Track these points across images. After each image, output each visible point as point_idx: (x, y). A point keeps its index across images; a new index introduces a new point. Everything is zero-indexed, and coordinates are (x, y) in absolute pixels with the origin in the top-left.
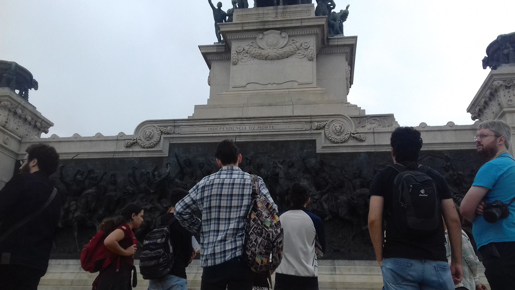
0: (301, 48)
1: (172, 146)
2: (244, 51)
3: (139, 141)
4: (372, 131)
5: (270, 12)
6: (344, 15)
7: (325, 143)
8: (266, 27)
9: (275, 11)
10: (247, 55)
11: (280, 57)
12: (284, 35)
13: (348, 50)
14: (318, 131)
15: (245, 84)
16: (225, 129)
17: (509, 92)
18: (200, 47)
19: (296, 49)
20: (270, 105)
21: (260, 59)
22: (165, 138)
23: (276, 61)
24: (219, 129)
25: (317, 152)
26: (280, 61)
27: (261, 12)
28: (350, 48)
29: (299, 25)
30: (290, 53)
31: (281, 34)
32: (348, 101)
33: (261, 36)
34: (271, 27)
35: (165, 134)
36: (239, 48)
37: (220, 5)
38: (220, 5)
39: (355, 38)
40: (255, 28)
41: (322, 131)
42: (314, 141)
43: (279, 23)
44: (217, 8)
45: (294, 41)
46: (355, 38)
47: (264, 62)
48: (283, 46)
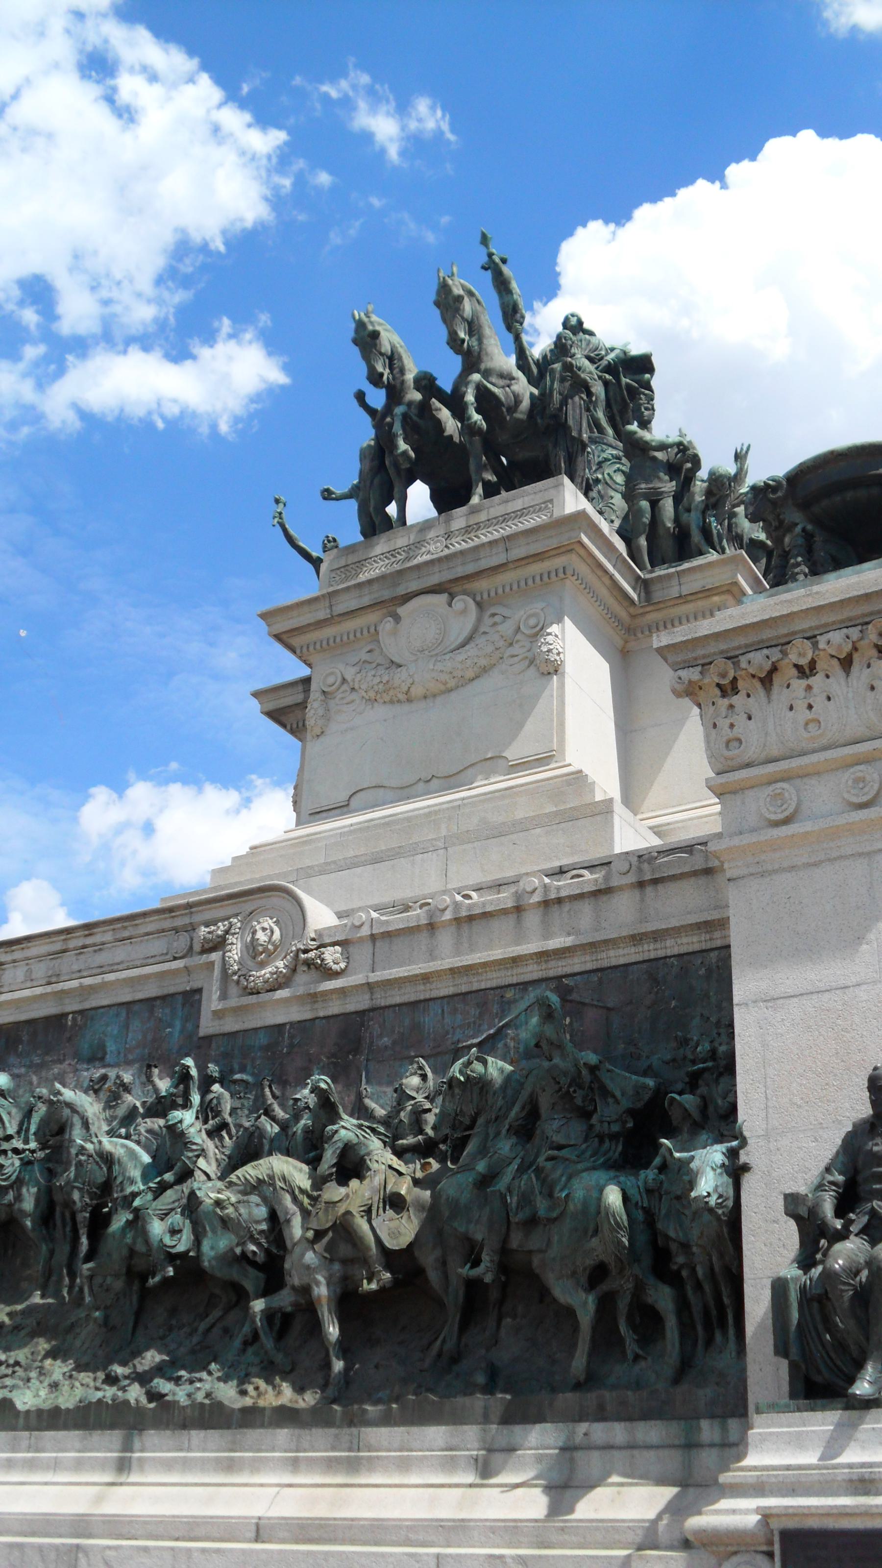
0: (519, 637)
2: (345, 687)
4: (365, 931)
7: (224, 996)
8: (401, 590)
10: (354, 696)
12: (459, 602)
14: (204, 958)
15: (342, 797)
17: (731, 706)
19: (501, 643)
20: (377, 859)
21: (392, 702)
25: (202, 1032)
29: (500, 559)
30: (483, 662)
33: (388, 624)
34: (414, 586)
36: (331, 680)
40: (366, 601)
41: (215, 956)
43: (436, 569)
45: (497, 619)
47: (406, 707)
48: (460, 640)
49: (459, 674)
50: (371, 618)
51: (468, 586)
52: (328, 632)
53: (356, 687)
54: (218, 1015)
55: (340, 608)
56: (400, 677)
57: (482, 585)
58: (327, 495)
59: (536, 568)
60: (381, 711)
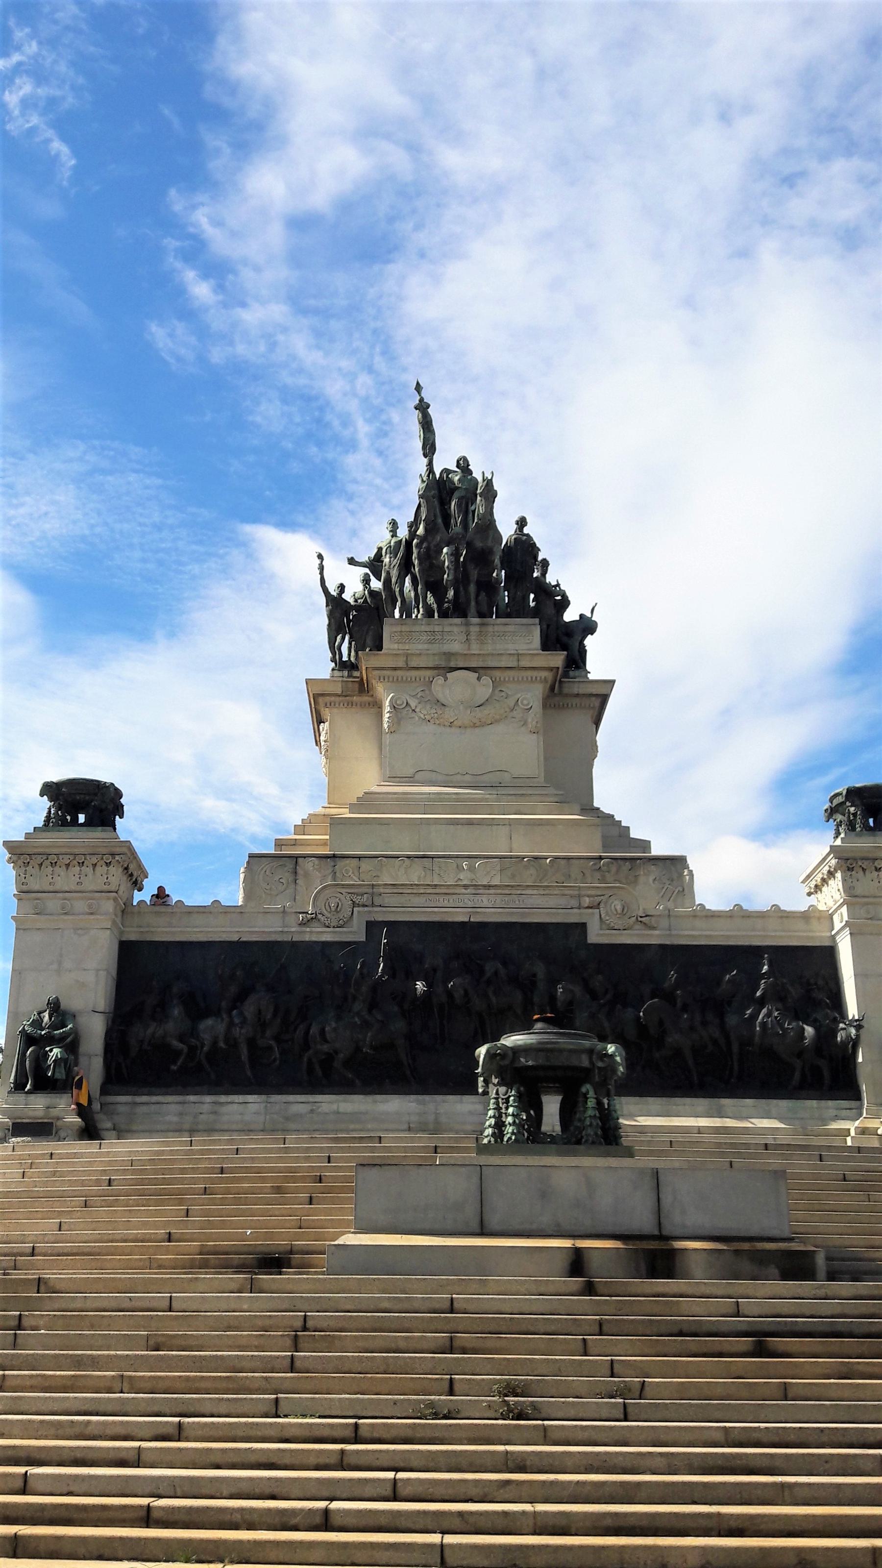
1: (371, 926)
3: (320, 916)
5: (456, 629)
6: (587, 626)
9: (463, 629)
10: (413, 715)
11: (478, 724)
12: (486, 680)
13: (597, 702)
15: (410, 772)
16: (451, 901)
19: (508, 710)
22: (359, 912)
23: (468, 730)
24: (441, 900)
25: (589, 941)
26: (477, 730)
27: (437, 628)
28: (599, 697)
29: (513, 664)
31: (479, 679)
32: (596, 805)
33: (440, 680)
35: (359, 906)
38: (342, 588)
39: (612, 682)
42: (583, 926)
44: (334, 592)
45: (503, 694)
47: (448, 730)
49: (483, 720)
50: (429, 673)
51: (489, 672)
53: (417, 710)
54: (598, 935)
55: (413, 664)
56: (449, 715)
57: (497, 674)
58: (352, 561)
59: (529, 673)
60: (431, 727)
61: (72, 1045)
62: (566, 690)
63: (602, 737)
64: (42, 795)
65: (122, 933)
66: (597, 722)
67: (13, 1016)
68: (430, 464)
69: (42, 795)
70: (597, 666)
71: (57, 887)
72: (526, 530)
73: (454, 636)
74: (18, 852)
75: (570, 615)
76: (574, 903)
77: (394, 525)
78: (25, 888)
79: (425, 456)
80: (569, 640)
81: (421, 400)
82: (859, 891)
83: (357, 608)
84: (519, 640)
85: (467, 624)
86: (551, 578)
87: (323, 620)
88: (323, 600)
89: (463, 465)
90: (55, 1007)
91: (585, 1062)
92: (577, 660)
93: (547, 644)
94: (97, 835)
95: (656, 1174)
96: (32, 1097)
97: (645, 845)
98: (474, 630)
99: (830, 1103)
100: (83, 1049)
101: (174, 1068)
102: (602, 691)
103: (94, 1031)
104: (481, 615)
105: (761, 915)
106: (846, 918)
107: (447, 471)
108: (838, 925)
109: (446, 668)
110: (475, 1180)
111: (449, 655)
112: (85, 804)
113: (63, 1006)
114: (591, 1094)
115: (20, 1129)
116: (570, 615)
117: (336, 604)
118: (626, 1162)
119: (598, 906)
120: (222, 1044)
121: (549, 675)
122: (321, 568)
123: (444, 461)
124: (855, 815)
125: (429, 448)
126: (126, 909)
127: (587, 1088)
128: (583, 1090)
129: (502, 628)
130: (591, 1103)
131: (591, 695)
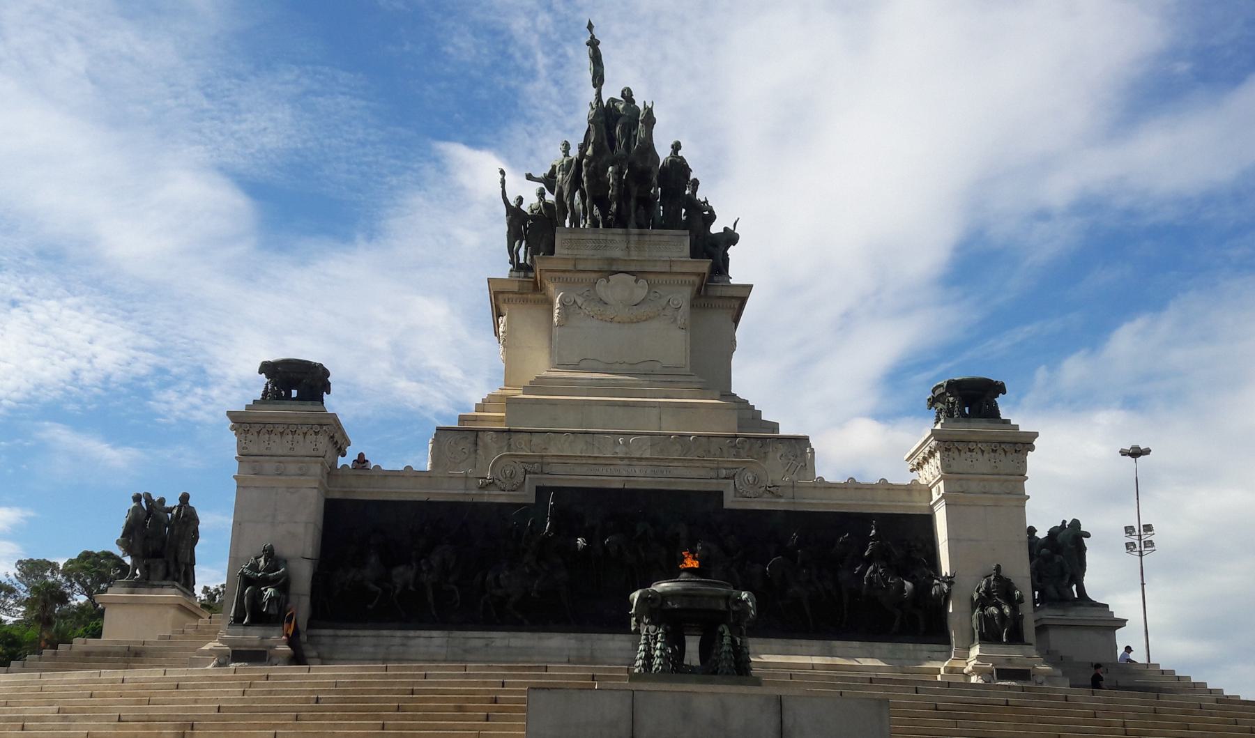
1: (541, 491)
5: (617, 238)
6: (730, 238)
8: (614, 268)
9: (624, 238)
12: (642, 282)
15: (576, 360)
18: (489, 280)
29: (667, 269)
31: (636, 281)
33: (603, 282)
37: (520, 200)
38: (520, 200)
39: (751, 286)
42: (721, 493)
44: (514, 205)
46: (751, 286)
50: (594, 275)
52: (568, 275)
55: (580, 267)
57: (652, 277)
59: (680, 278)
61: (284, 586)
62: (711, 293)
63: (739, 334)
64: (260, 372)
65: (327, 492)
66: (736, 321)
67: (234, 560)
68: (599, 94)
69: (260, 372)
70: (737, 273)
71: (273, 451)
72: (680, 153)
73: (617, 244)
74: (240, 422)
75: (716, 228)
76: (713, 474)
77: (567, 147)
78: (245, 452)
79: (595, 86)
80: (714, 249)
81: (593, 37)
82: (954, 469)
83: (533, 217)
84: (673, 248)
85: (628, 234)
86: (700, 196)
87: (504, 228)
88: (504, 210)
89: (627, 95)
90: (269, 553)
91: (722, 606)
92: (721, 267)
93: (695, 253)
94: (306, 409)
95: (780, 700)
96: (249, 629)
97: (774, 426)
98: (634, 239)
99: (924, 646)
100: (293, 588)
101: (370, 607)
102: (741, 294)
103: (303, 574)
104: (640, 226)
105: (871, 488)
106: (942, 491)
107: (613, 100)
108: (935, 497)
109: (609, 271)
110: (629, 701)
111: (612, 261)
112: (297, 381)
113: (278, 551)
114: (727, 632)
115: (238, 655)
116: (716, 228)
117: (515, 213)
118: (755, 690)
119: (733, 477)
120: (411, 588)
121: (697, 280)
122: (503, 182)
123: (611, 91)
124: (953, 404)
125: (598, 80)
126: (332, 472)
127: (724, 628)
128: (720, 629)
129: (657, 238)
130: (726, 640)
131: (733, 297)
